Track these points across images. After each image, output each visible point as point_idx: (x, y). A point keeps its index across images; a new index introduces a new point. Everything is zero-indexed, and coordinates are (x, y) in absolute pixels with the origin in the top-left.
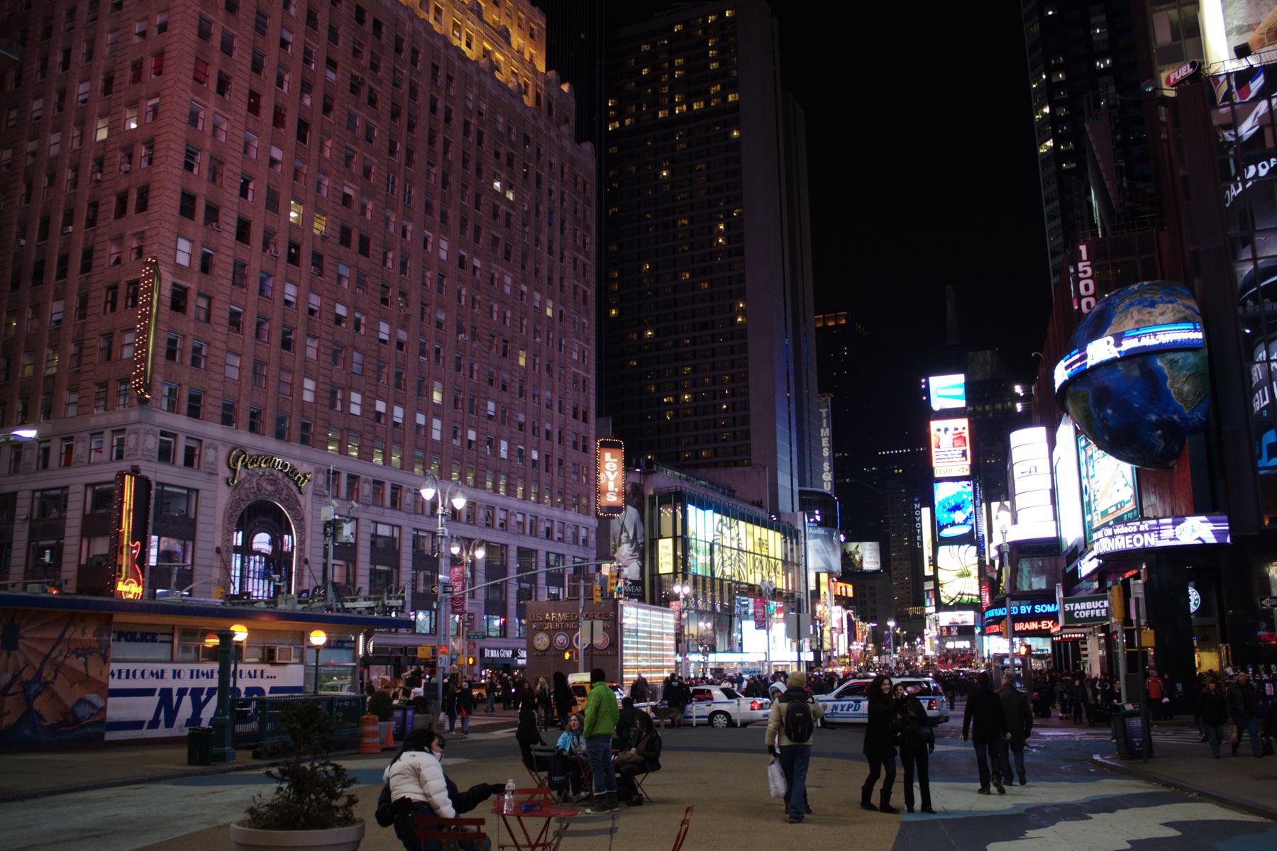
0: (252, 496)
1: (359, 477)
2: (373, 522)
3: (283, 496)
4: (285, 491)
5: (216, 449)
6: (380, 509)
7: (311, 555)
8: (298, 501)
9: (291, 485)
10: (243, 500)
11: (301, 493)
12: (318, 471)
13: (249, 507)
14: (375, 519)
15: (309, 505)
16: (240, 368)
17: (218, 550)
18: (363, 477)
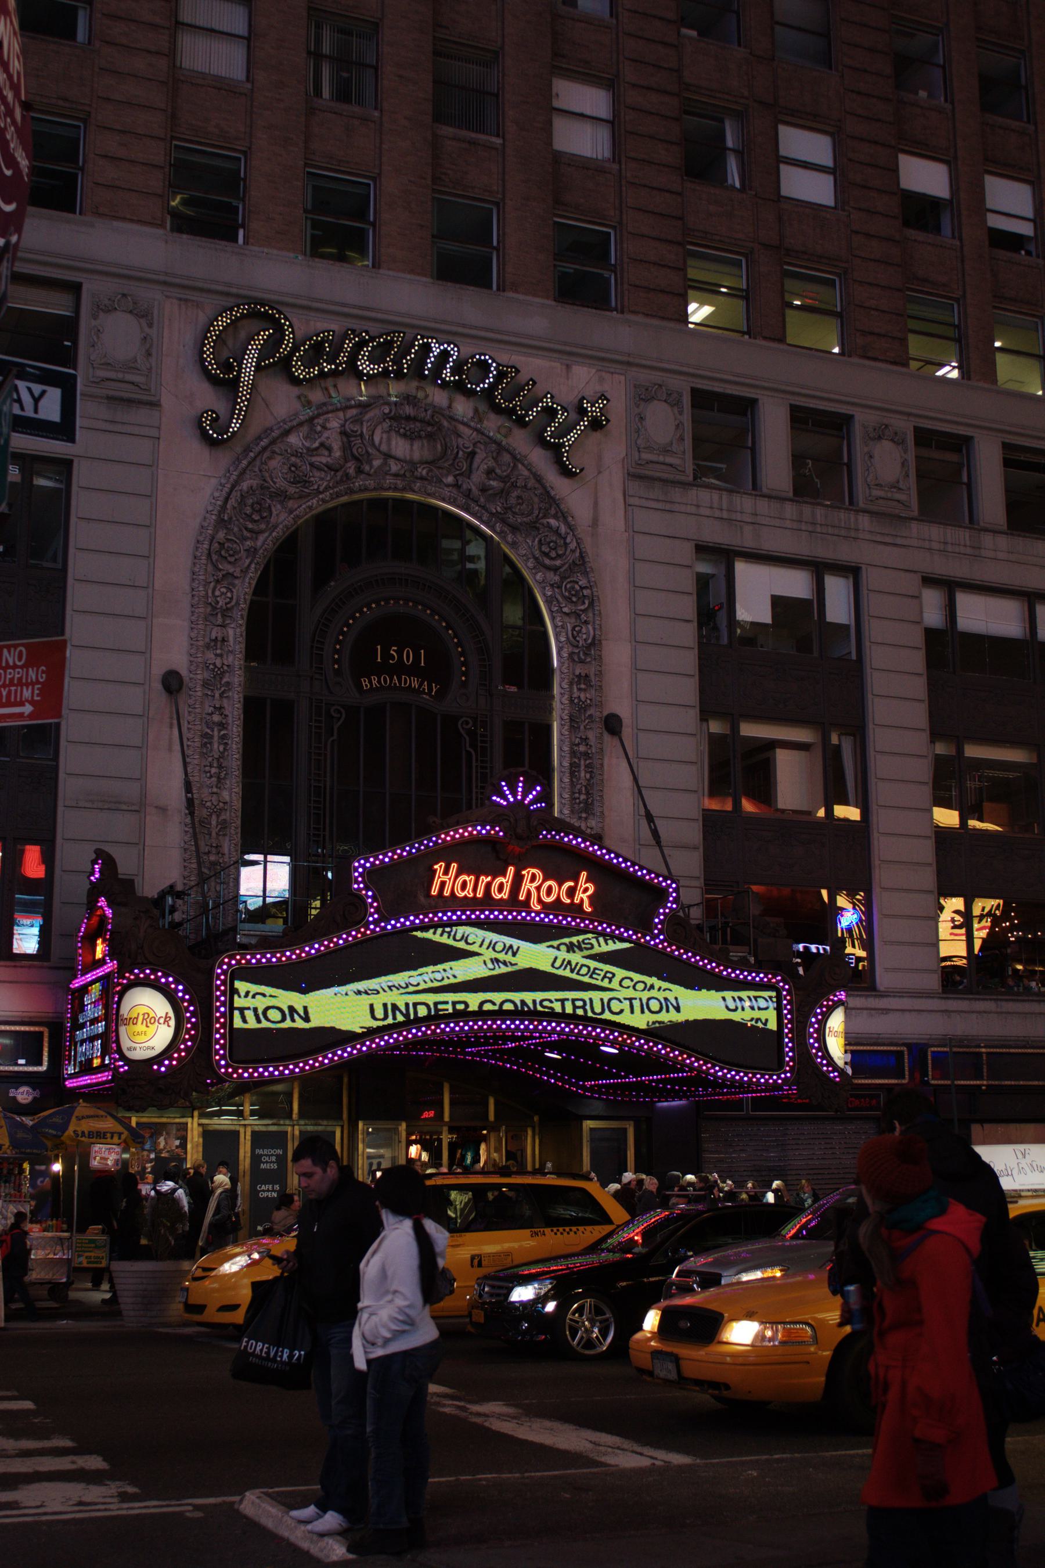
0: (319, 479)
1: (849, 419)
2: (929, 581)
3: (478, 477)
4: (482, 462)
5: (143, 314)
6: (964, 535)
7: (637, 701)
8: (551, 502)
9: (520, 441)
10: (282, 496)
11: (566, 472)
12: (644, 395)
13: (323, 523)
14: (942, 567)
15: (613, 520)
16: (249, 40)
17: (172, 683)
18: (863, 419)
